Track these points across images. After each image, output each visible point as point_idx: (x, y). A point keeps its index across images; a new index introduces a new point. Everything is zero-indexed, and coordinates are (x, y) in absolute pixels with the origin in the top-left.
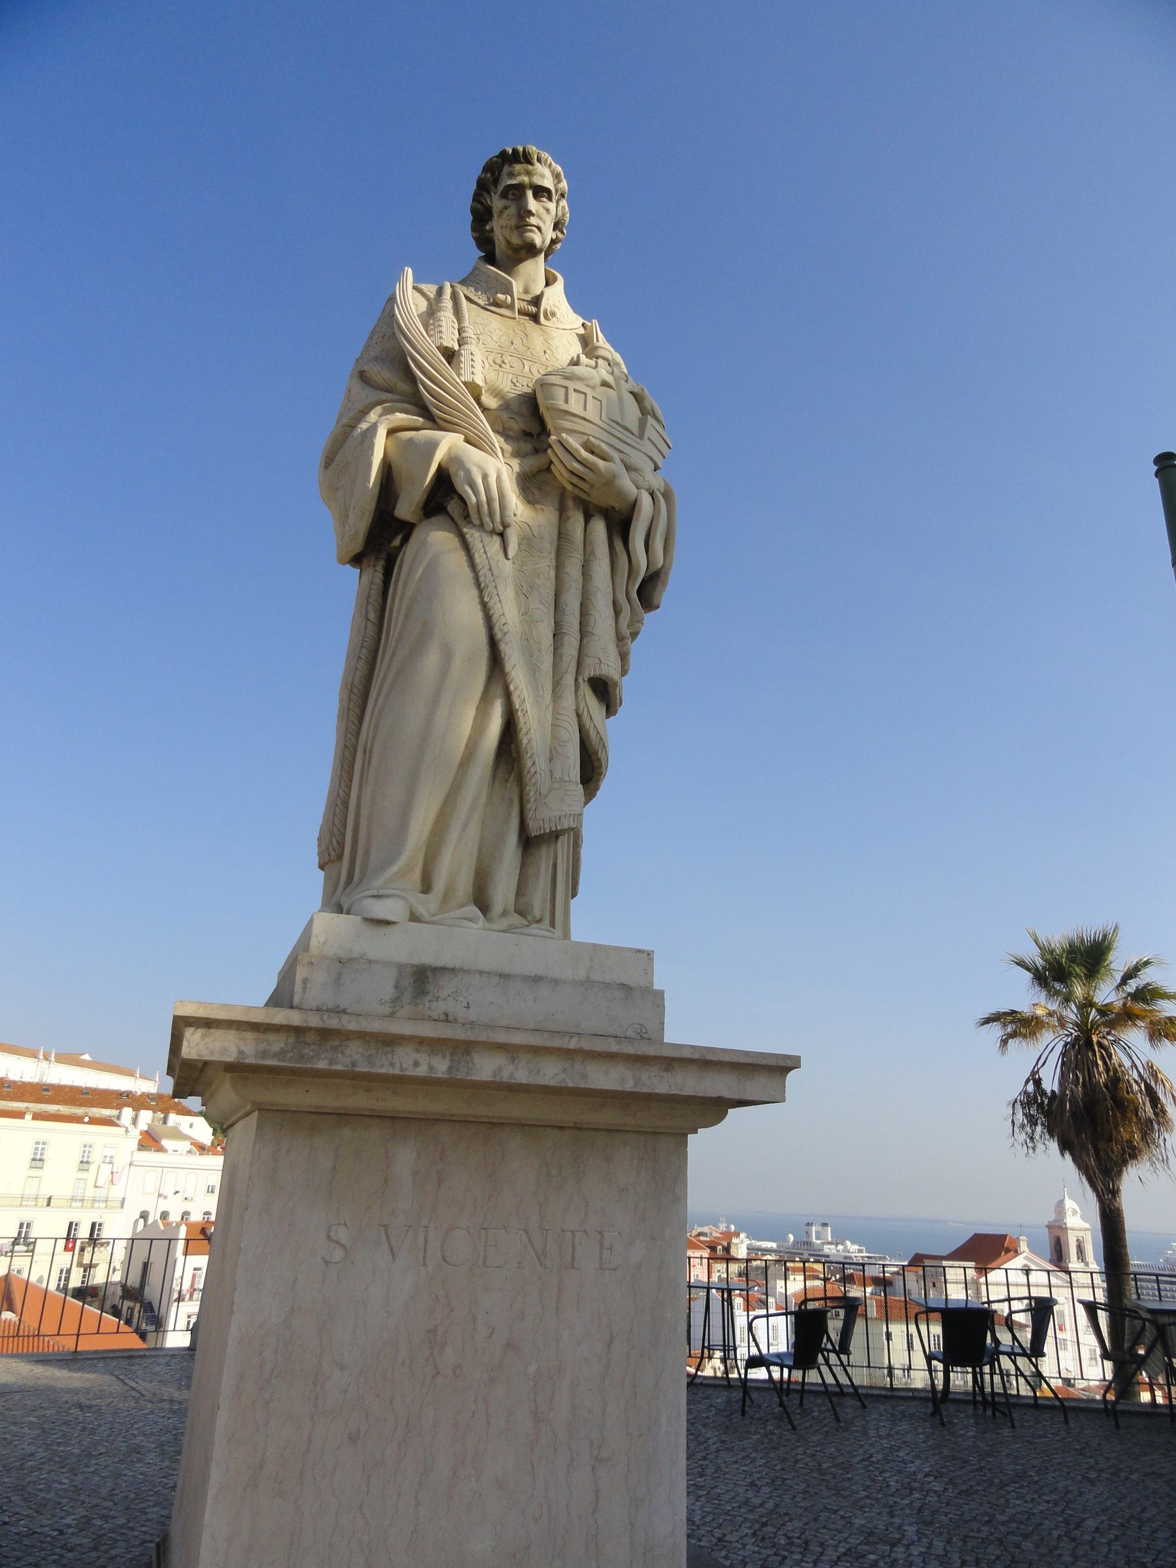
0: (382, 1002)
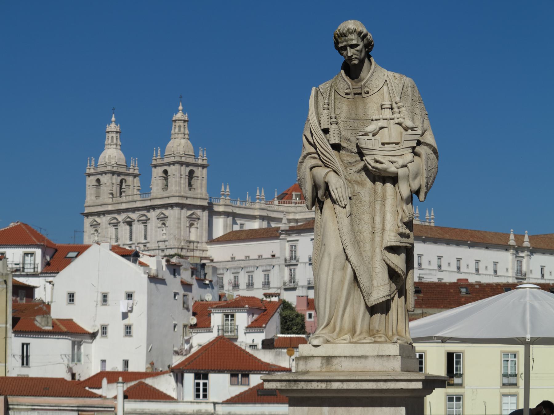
0: (318, 368)
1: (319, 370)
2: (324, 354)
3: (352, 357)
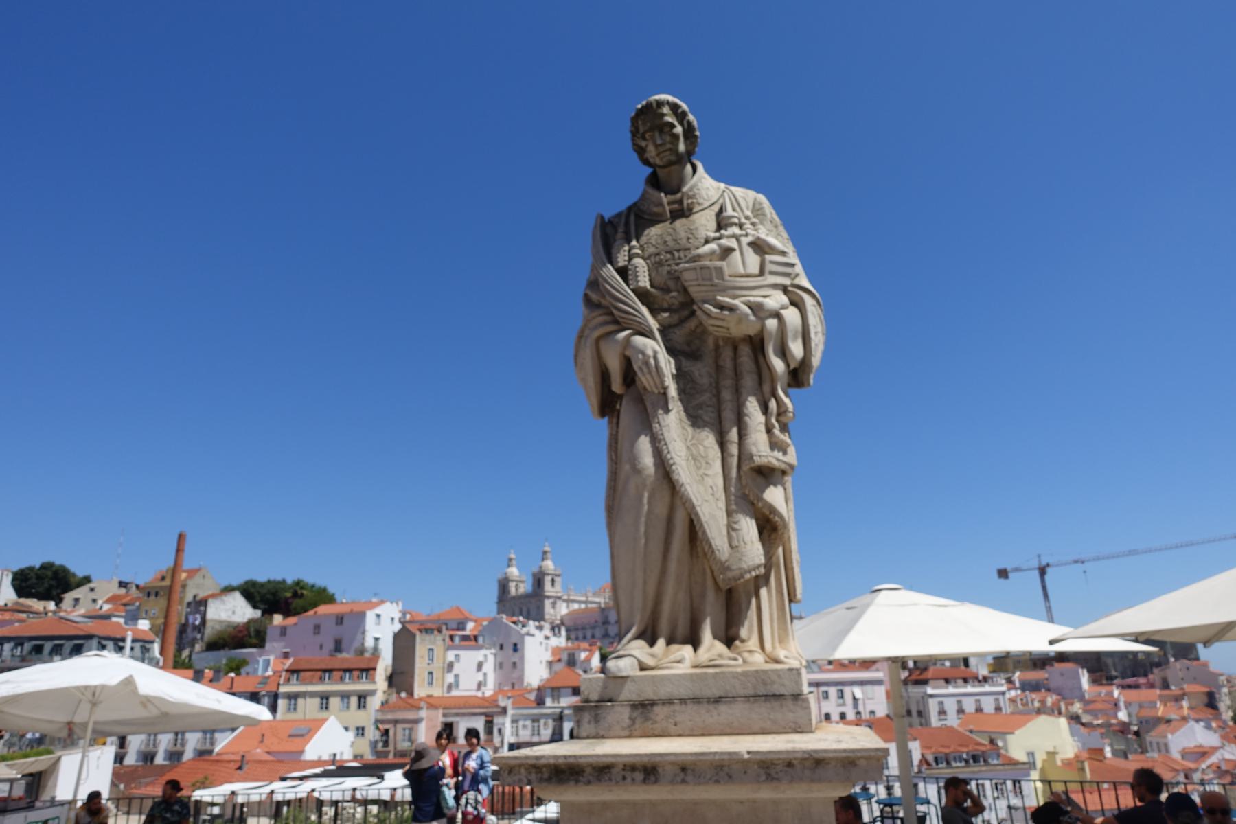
1: (627, 733)
2: (634, 697)
3: (696, 700)
